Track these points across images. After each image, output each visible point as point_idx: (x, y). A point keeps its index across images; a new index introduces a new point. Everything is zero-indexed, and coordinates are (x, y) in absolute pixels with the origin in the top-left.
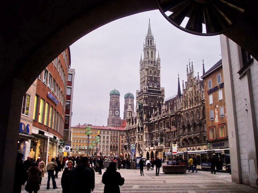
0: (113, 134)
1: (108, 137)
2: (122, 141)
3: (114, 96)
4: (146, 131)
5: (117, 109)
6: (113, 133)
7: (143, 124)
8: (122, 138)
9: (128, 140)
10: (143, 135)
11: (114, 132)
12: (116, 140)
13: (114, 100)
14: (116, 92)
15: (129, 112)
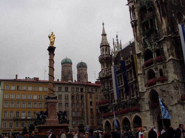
0: (75, 91)
1: (67, 97)
2: (91, 103)
3: (66, 64)
4: (173, 56)
5: (70, 78)
6: (75, 89)
7: (160, 43)
8: (91, 97)
9: (109, 96)
10: (165, 67)
11: (78, 87)
12: (80, 102)
13: (67, 69)
14: (67, 61)
15: (104, 47)
